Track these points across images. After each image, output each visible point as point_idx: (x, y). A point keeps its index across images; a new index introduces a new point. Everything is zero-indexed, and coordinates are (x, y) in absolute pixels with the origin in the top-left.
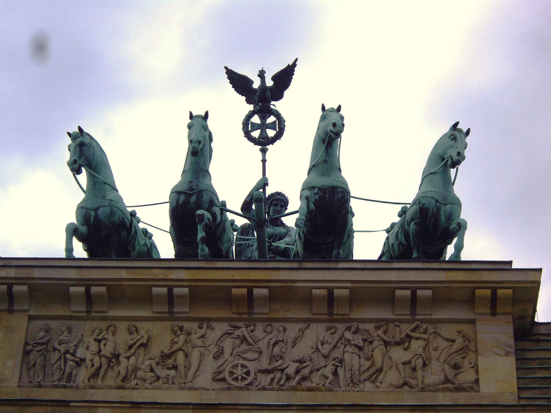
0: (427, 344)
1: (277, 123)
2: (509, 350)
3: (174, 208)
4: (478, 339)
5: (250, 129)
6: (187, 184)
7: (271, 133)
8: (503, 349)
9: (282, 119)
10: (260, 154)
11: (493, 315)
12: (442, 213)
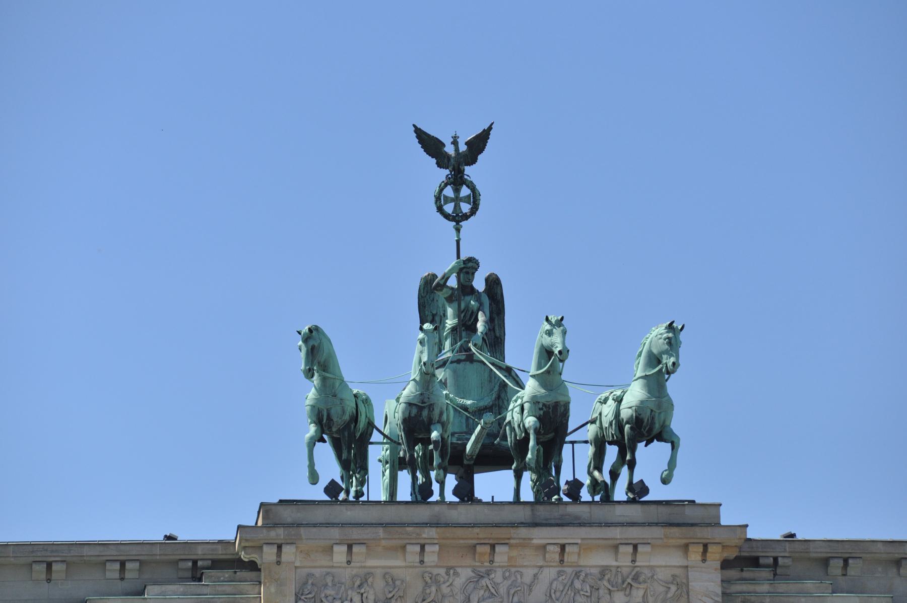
0: (645, 593)
1: (472, 195)
2: (716, 599)
3: (405, 418)
4: (690, 587)
5: (442, 202)
6: (418, 396)
7: (465, 208)
8: (712, 599)
9: (477, 192)
10: (454, 232)
11: (704, 561)
12: (657, 421)
